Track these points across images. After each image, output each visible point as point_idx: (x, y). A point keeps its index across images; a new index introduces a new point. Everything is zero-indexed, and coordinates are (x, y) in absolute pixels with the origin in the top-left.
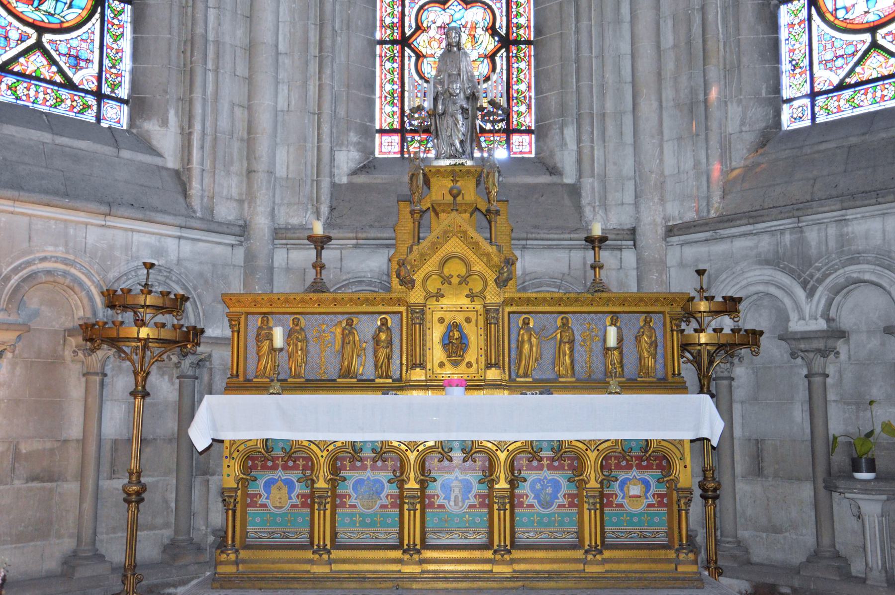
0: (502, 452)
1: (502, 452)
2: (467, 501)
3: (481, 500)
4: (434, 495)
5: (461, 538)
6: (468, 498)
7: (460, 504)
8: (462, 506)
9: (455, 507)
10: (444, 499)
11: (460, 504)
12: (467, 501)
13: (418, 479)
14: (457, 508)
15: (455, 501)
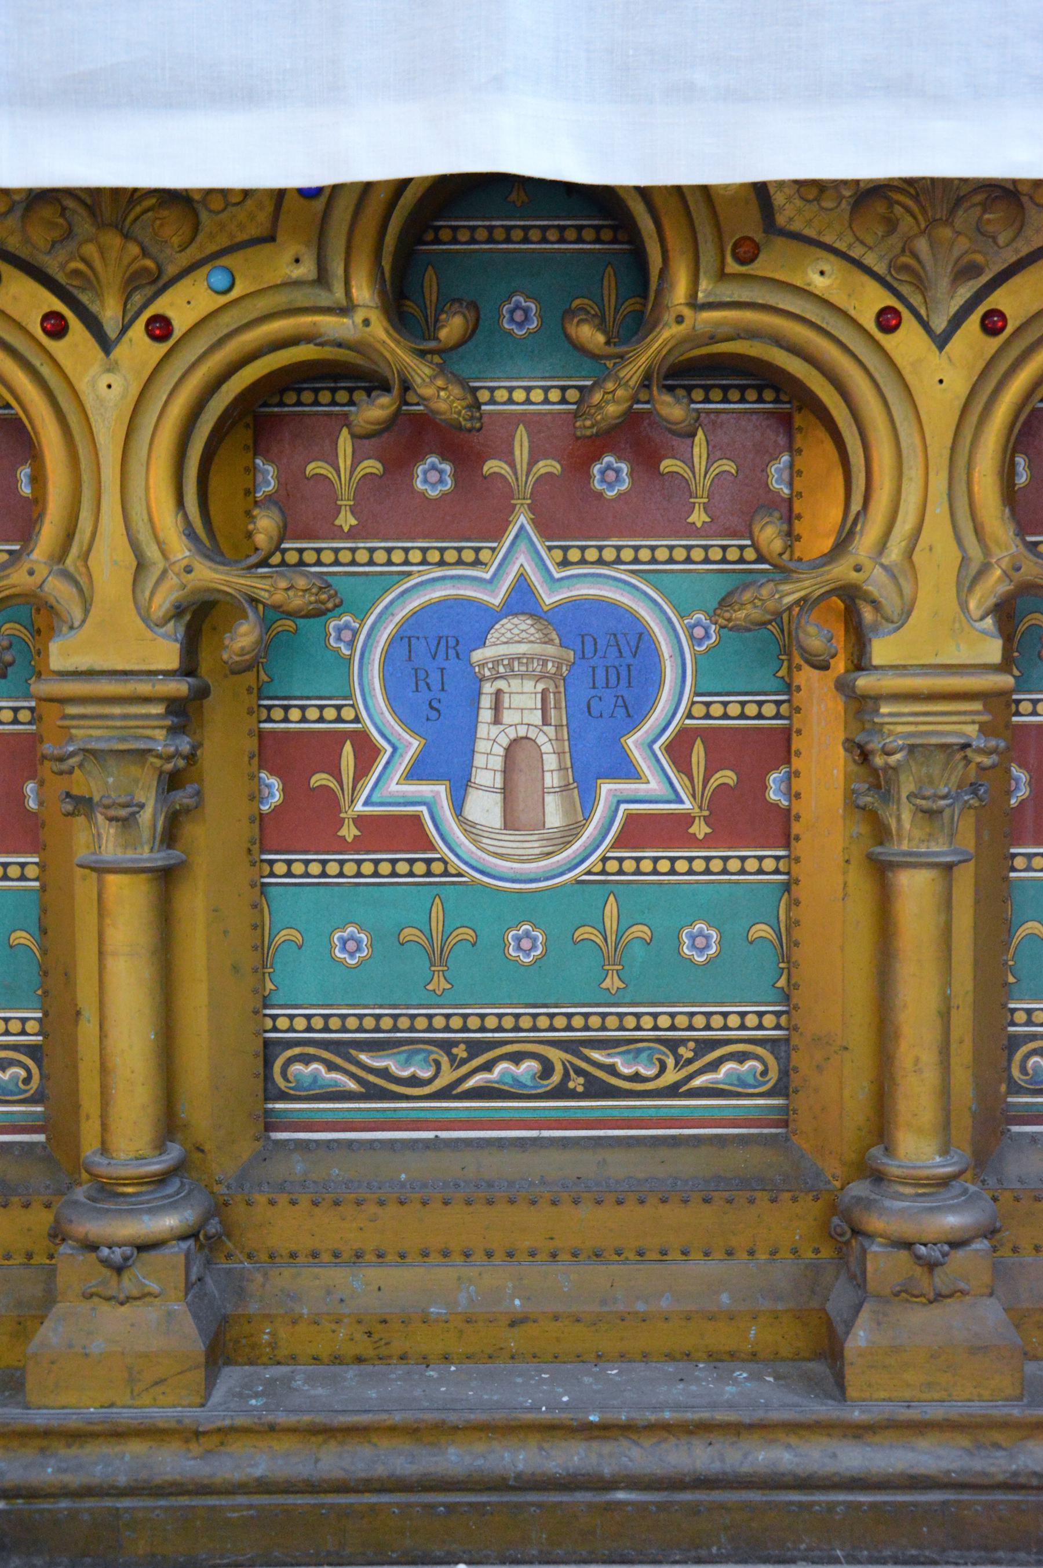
0: (941, 341)
1: (941, 341)
2: (606, 788)
3: (727, 777)
4: (340, 738)
5: (561, 1092)
6: (627, 771)
7: (554, 816)
8: (570, 833)
9: (511, 842)
10: (416, 773)
11: (554, 816)
12: (606, 788)
13: (162, 601)
14: (533, 846)
15: (507, 791)
